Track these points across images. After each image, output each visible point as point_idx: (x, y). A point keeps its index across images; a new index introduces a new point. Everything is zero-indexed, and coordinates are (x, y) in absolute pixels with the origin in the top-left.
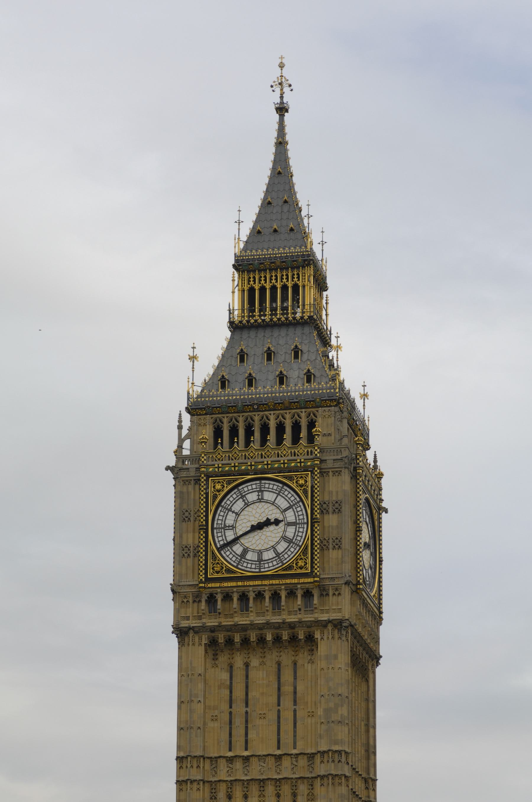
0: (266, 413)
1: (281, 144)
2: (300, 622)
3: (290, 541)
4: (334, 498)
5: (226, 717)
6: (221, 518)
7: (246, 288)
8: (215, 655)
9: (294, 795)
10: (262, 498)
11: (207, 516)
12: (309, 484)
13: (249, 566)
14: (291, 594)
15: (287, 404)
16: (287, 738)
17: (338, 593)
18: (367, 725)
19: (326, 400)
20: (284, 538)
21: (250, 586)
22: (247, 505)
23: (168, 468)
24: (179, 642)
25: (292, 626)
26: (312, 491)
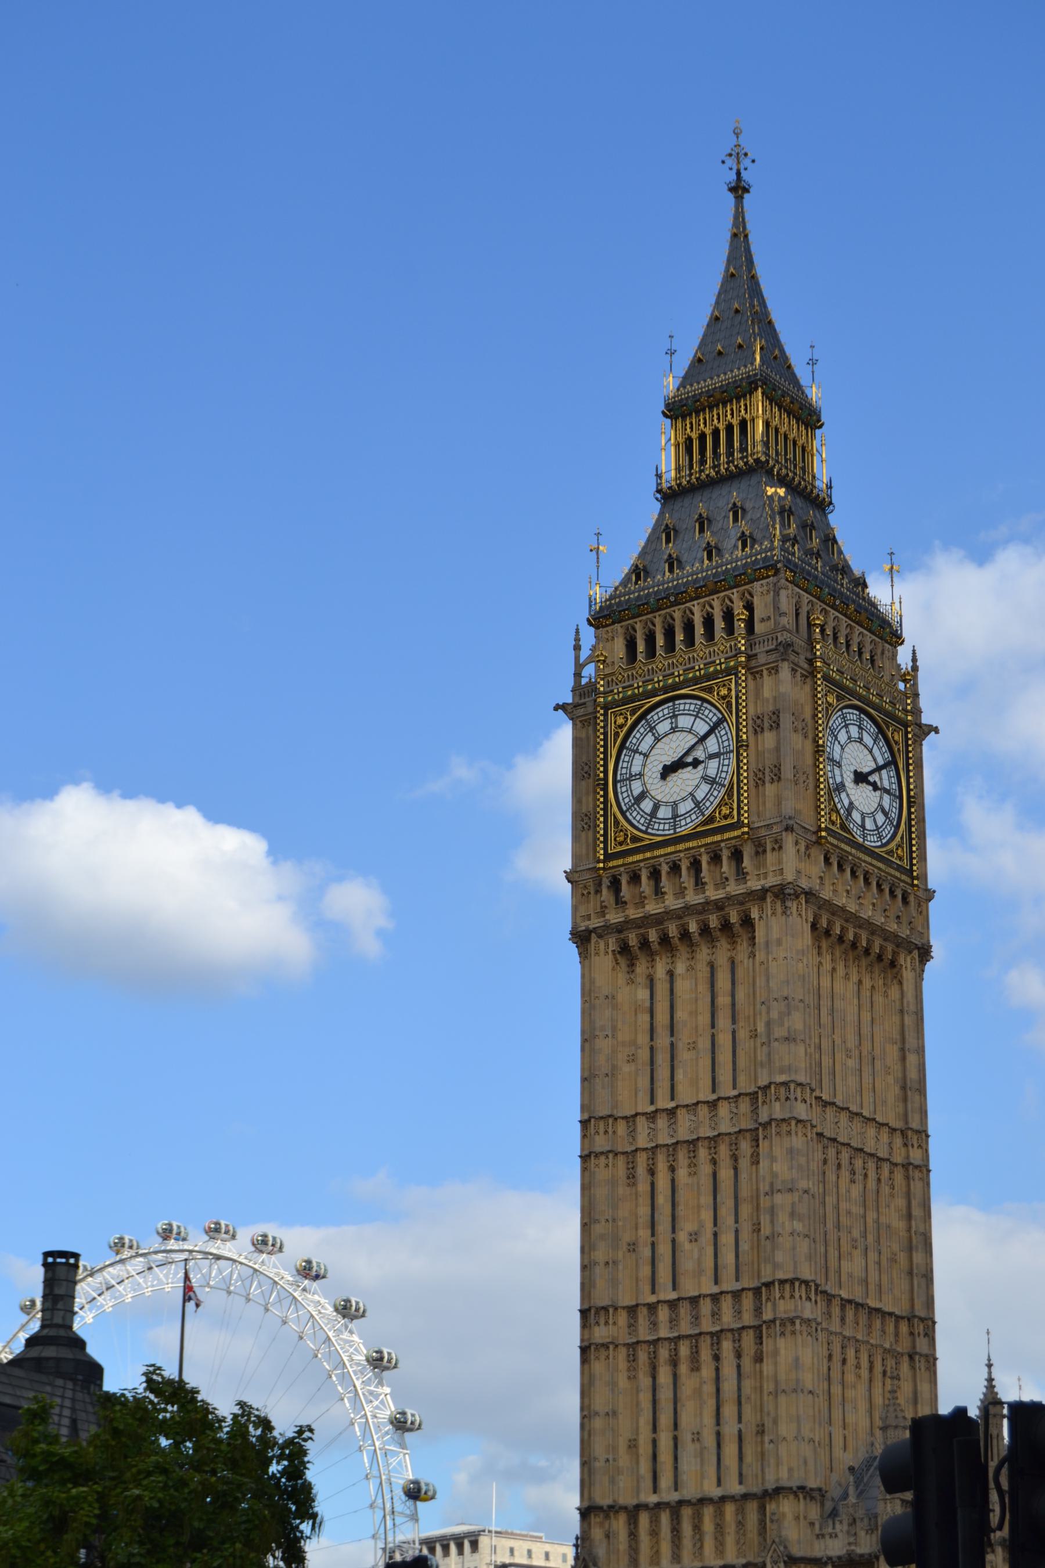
0: (687, 605)
2: (728, 898)
3: (712, 782)
4: (771, 708)
5: (644, 1055)
6: (625, 765)
7: (681, 440)
8: (631, 965)
9: (735, 1158)
10: (677, 727)
11: (606, 766)
12: (733, 693)
13: (661, 827)
14: (716, 859)
15: (711, 586)
16: (725, 1075)
17: (779, 846)
18: (902, 1050)
19: (760, 569)
20: (705, 778)
21: (661, 856)
22: (658, 740)
23: (557, 708)
24: (580, 954)
25: (719, 906)
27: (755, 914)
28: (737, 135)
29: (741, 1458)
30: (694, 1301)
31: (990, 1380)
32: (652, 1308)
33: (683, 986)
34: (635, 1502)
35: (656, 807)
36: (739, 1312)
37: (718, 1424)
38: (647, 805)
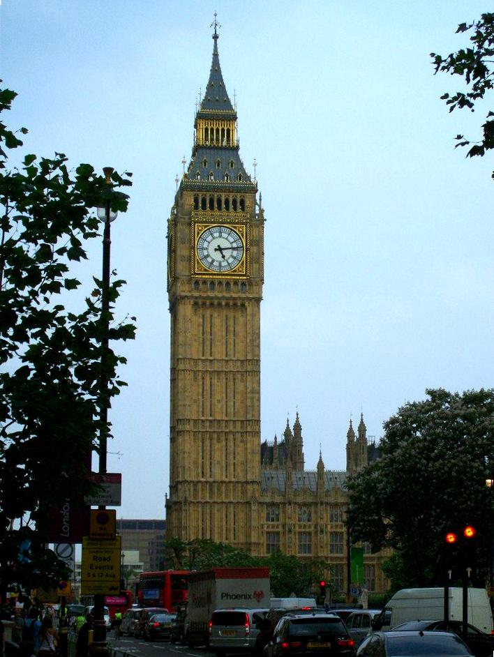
1: (216, 55)
3: (235, 258)
5: (201, 339)
11: (194, 242)
25: (235, 299)
26: (246, 235)
27: (247, 304)
28: (216, 15)
29: (234, 471)
30: (219, 421)
31: (321, 457)
32: (203, 421)
33: (217, 321)
34: (196, 480)
35: (213, 261)
36: (235, 427)
37: (226, 459)
38: (210, 260)
